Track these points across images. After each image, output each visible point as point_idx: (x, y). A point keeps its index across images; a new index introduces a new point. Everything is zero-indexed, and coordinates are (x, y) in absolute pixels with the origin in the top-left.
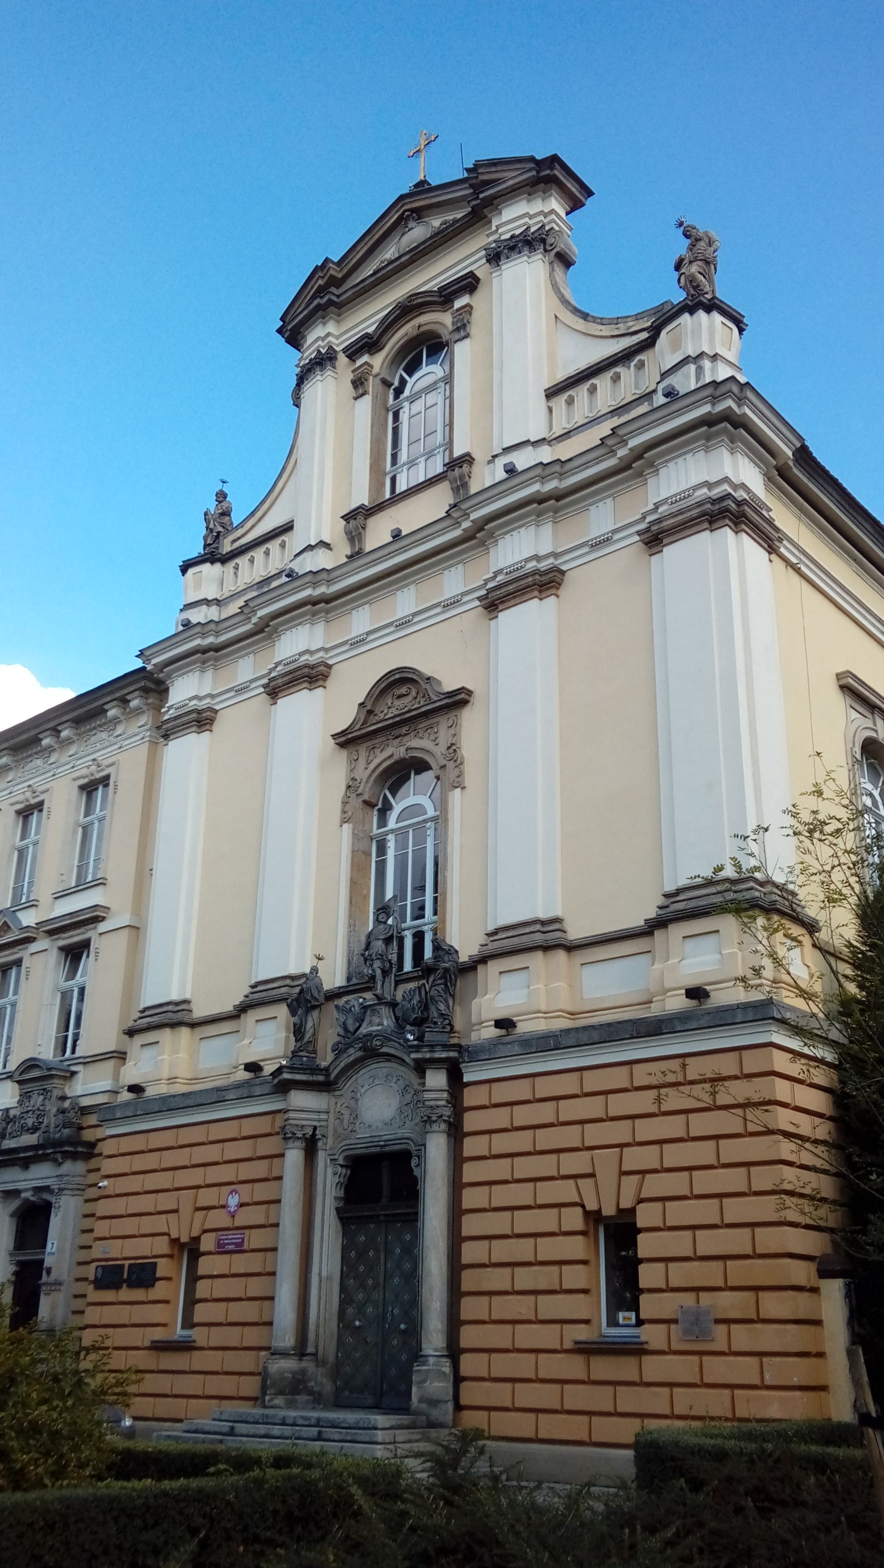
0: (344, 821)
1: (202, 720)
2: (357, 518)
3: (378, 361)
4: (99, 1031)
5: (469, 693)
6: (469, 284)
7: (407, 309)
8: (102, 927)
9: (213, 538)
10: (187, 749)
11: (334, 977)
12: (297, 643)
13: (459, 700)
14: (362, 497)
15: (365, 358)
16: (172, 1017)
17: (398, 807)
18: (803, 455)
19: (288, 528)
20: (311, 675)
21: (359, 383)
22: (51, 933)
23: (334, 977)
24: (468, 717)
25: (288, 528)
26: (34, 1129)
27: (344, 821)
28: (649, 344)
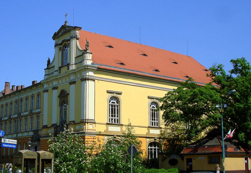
0: (59, 106)
1: (47, 91)
2: (60, 68)
3: (62, 46)
4: (41, 127)
5: (69, 94)
6: (69, 40)
7: (64, 41)
8: (40, 114)
9: (48, 65)
10: (46, 94)
11: (58, 124)
12: (55, 83)
13: (68, 94)
14: (60, 65)
15: (60, 46)
16: (45, 127)
17: (64, 105)
18: (98, 68)
19: (54, 67)
20: (55, 88)
21: (60, 49)
22: (36, 114)
23: (58, 124)
24: (69, 96)
25: (54, 67)
26: (35, 138)
27: (59, 106)
28: (82, 55)
